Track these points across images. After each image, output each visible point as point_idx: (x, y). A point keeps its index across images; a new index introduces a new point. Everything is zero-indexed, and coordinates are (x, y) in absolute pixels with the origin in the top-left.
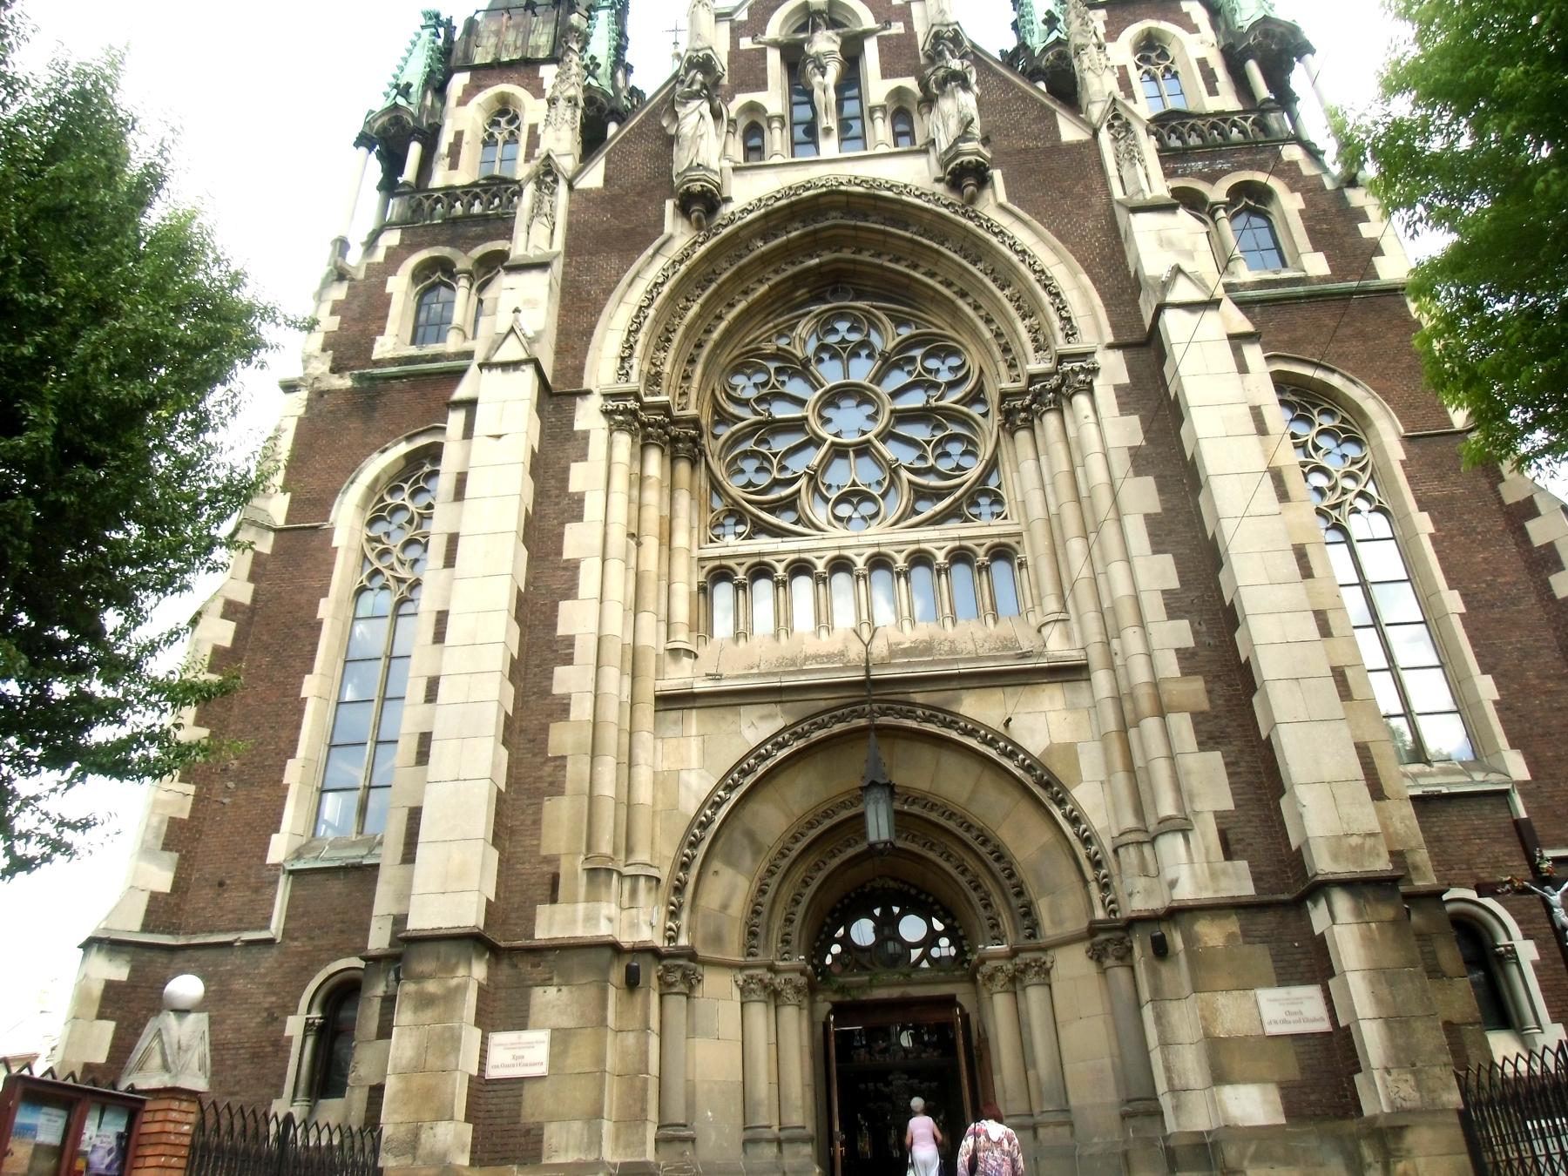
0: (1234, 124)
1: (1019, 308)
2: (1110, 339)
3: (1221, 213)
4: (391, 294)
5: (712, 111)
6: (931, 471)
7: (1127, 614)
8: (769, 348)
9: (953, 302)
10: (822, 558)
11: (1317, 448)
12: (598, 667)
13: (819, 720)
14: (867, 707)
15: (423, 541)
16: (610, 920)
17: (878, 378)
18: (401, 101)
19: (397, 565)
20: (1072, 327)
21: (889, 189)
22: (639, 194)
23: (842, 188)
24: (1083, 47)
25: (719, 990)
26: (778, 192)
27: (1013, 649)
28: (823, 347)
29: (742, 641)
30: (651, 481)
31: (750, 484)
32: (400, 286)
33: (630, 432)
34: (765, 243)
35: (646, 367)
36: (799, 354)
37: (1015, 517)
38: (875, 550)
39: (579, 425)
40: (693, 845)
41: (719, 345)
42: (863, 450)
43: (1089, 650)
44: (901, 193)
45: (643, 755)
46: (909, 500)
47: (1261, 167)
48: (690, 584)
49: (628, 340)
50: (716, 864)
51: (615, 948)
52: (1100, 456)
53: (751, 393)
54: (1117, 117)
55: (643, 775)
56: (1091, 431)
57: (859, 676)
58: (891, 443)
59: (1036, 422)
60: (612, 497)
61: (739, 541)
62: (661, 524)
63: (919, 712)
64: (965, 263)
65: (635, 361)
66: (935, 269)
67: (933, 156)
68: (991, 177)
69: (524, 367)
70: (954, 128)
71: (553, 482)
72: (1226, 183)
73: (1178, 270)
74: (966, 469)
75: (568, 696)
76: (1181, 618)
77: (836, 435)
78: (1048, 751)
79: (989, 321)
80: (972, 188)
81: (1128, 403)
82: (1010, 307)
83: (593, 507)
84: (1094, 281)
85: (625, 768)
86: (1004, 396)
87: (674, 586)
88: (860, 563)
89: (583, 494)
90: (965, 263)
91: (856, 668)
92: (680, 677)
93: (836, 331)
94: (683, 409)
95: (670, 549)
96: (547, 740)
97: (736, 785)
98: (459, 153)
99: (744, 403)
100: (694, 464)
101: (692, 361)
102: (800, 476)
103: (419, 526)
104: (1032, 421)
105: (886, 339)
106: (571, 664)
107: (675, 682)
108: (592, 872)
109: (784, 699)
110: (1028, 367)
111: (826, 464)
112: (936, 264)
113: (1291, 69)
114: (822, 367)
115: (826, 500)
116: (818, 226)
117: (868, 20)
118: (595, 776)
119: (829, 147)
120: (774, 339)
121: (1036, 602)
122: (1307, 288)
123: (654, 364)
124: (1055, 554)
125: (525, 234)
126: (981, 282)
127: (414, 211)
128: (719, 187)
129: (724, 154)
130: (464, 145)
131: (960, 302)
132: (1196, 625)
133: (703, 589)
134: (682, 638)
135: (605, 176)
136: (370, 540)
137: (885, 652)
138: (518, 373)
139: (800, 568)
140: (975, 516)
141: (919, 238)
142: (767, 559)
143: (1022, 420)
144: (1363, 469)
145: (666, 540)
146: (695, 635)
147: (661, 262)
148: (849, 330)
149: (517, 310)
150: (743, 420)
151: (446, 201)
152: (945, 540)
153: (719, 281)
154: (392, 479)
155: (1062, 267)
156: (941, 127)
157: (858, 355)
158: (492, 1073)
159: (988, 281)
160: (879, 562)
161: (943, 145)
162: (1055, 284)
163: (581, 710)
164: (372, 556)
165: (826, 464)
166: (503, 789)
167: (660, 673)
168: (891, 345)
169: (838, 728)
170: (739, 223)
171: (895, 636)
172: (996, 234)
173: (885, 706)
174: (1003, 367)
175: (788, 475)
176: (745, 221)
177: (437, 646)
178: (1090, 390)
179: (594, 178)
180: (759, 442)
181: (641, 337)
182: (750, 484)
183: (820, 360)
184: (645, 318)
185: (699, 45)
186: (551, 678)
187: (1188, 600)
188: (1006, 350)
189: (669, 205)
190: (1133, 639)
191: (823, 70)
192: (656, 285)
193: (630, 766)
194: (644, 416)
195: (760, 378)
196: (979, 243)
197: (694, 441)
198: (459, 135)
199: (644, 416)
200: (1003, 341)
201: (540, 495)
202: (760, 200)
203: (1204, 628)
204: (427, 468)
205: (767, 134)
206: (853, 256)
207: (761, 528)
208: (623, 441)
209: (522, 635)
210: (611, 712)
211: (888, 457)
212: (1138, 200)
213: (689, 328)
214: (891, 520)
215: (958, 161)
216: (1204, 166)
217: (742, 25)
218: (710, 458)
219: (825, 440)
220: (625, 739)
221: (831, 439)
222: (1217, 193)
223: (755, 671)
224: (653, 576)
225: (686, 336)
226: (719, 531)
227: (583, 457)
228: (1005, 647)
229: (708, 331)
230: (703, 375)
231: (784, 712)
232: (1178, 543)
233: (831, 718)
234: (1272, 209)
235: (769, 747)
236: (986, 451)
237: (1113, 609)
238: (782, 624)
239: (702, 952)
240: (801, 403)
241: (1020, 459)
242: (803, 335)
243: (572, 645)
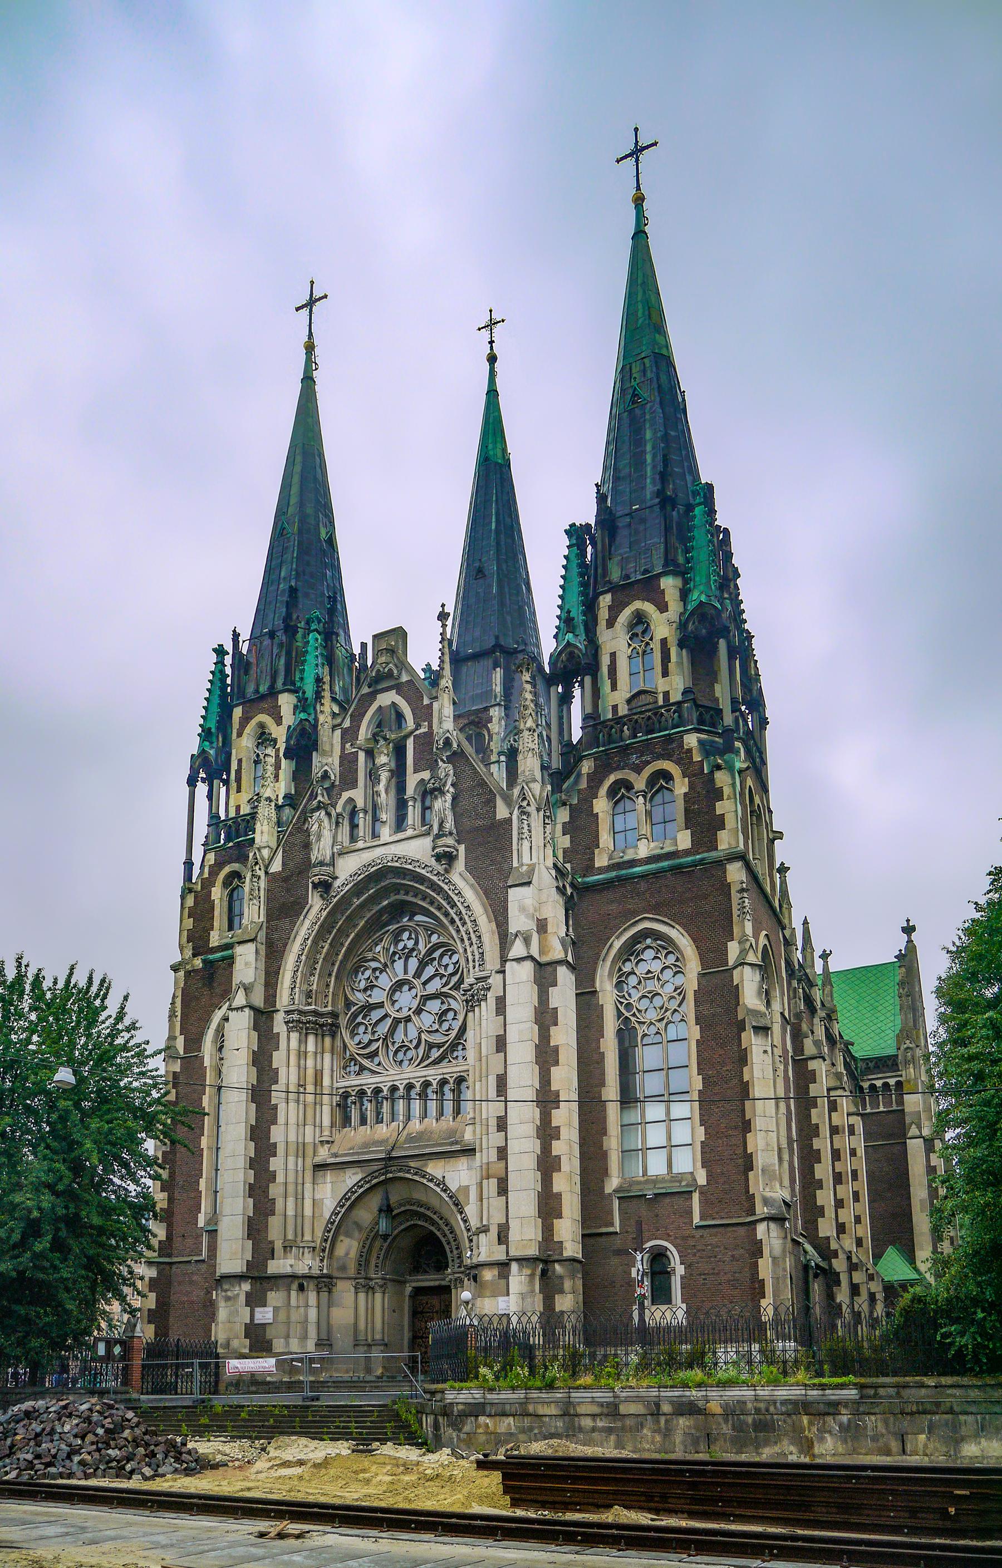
3: (641, 799)
6: (437, 1031)
11: (659, 979)
16: (291, 1266)
17: (418, 974)
25: (345, 1290)
28: (394, 953)
38: (407, 1081)
40: (329, 1232)
42: (408, 1019)
45: (308, 1195)
50: (341, 1238)
51: (294, 1277)
78: (458, 1190)
85: (300, 1201)
92: (324, 1154)
94: (326, 1007)
97: (344, 1205)
101: (330, 975)
108: (285, 1247)
133: (338, 1105)
158: (256, 1322)
163: (280, 1178)
179: (276, 867)
180: (364, 1018)
207: (363, 1068)
208: (294, 1036)
210: (291, 1179)
214: (416, 1063)
220: (300, 1187)
222: (640, 783)
227: (277, 1048)
229: (338, 955)
230: (337, 977)
239: (336, 1274)
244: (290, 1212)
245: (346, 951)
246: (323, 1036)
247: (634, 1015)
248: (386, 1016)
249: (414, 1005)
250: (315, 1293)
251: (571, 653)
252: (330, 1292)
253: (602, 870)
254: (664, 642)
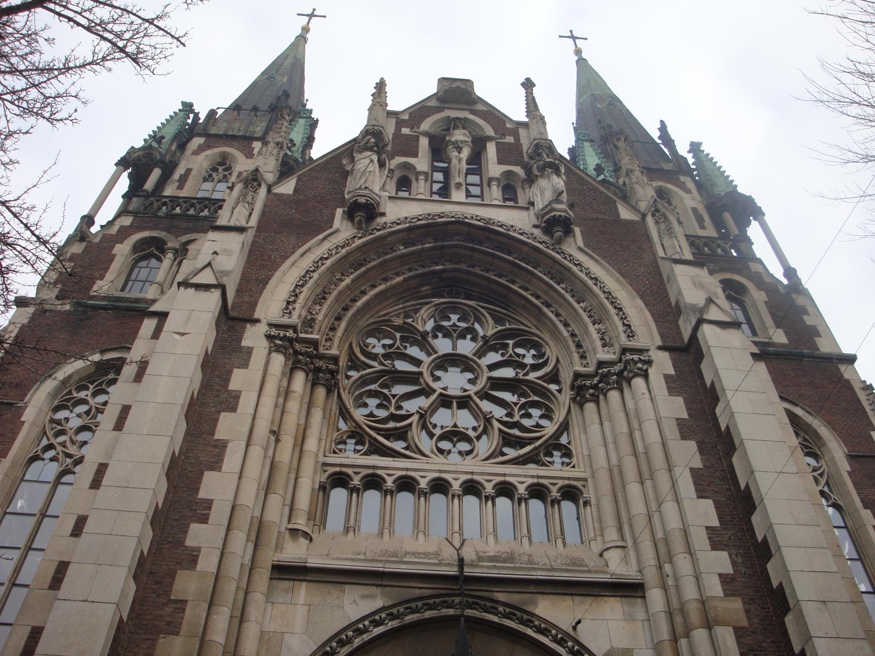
0: (719, 246)
1: (590, 317)
2: (660, 343)
4: (115, 255)
5: (379, 161)
6: (517, 425)
7: (678, 544)
8: (398, 321)
9: (539, 309)
10: (425, 477)
12: (228, 529)
13: (413, 605)
14: (457, 600)
15: (94, 428)
18: (155, 144)
19: (68, 444)
20: (632, 331)
21: (500, 226)
22: (318, 202)
23: (466, 220)
24: (632, 171)
26: (420, 215)
27: (581, 566)
28: (438, 328)
29: (351, 534)
30: (294, 394)
31: (371, 415)
32: (123, 250)
33: (285, 354)
34: (406, 248)
35: (304, 313)
36: (420, 328)
37: (582, 466)
38: (469, 477)
39: (245, 343)
41: (361, 312)
42: (464, 402)
43: (645, 571)
44: (508, 230)
45: (253, 613)
46: (498, 444)
47: (739, 272)
48: (313, 482)
49: (294, 291)
52: (655, 423)
53: (379, 350)
54: (657, 210)
55: (251, 632)
56: (646, 404)
57: (453, 571)
58: (485, 401)
59: (601, 397)
60: (263, 399)
61: (357, 455)
62: (297, 430)
63: (501, 609)
64: (551, 282)
65: (297, 306)
66: (527, 285)
67: (532, 212)
68: (573, 229)
69: (213, 290)
70: (549, 196)
71: (217, 379)
73: (710, 301)
74: (544, 427)
75: (198, 550)
76: (722, 550)
77: (444, 389)
79: (566, 325)
80: (560, 233)
81: (674, 388)
82: (584, 315)
83: (246, 404)
84: (646, 305)
85: (237, 621)
86: (577, 376)
87: (300, 480)
88: (456, 486)
89: (240, 392)
90: (551, 282)
91: (449, 565)
93: (449, 319)
94: (327, 349)
95: (301, 451)
96: (172, 584)
98: (186, 181)
99: (374, 357)
100: (329, 391)
101: (339, 318)
102: (412, 415)
103: (94, 417)
104: (598, 397)
105: (488, 329)
106: (206, 523)
107: (291, 556)
109: (384, 583)
110: (598, 356)
111: (433, 409)
112: (529, 283)
113: (749, 223)
114: (435, 341)
115: (431, 435)
116: (445, 243)
117: (489, 131)
118: (210, 623)
119: (458, 195)
120: (402, 316)
121: (598, 533)
122: (774, 349)
123: (311, 313)
124: (615, 496)
125: (229, 213)
126: (562, 296)
127: (146, 208)
128: (378, 204)
129: (383, 188)
130: (191, 178)
131: (545, 309)
132: (734, 556)
134: (301, 522)
135: (295, 188)
136: (52, 421)
137: (474, 557)
138: (207, 294)
139: (407, 484)
140: (549, 462)
141: (519, 262)
142: (379, 472)
143: (590, 395)
144: (821, 475)
145: (299, 443)
146: (312, 523)
147: (327, 245)
148: (459, 320)
149: (215, 253)
150: (371, 367)
151: (170, 204)
152: (526, 476)
153: (368, 266)
154: (82, 379)
155: (624, 293)
156: (539, 195)
157: (465, 338)
159: (568, 296)
160: (472, 488)
161: (539, 205)
162: (618, 302)
163: (207, 563)
164: (50, 434)
165: (433, 409)
166: (125, 618)
167: (278, 547)
168: (490, 333)
169: (428, 614)
170: (389, 230)
171: (481, 547)
172: (576, 265)
173: (471, 600)
174: (576, 357)
175: (403, 412)
176: (393, 229)
177: (92, 491)
178: (646, 376)
179: (287, 188)
180: (383, 386)
181: (305, 290)
182: (371, 415)
183: (435, 337)
184: (310, 278)
185: (375, 123)
186: (186, 532)
187: (727, 537)
188: (579, 346)
189: (339, 212)
190: (683, 563)
191: (460, 150)
192: (321, 259)
193: (241, 621)
194: (298, 346)
195: (388, 342)
196: (562, 270)
197: (333, 373)
198: (189, 171)
199: (298, 346)
200: (577, 339)
201: (205, 387)
202: (406, 218)
203: (740, 561)
204: (111, 376)
205: (414, 184)
206: (467, 268)
208: (278, 360)
209: (168, 491)
210: (233, 569)
211: (484, 410)
212: (677, 257)
213: (340, 293)
215: (552, 214)
217: (404, 121)
218: (341, 391)
219: (434, 391)
220: (241, 596)
221: (439, 391)
223: (362, 557)
224: (285, 467)
225: (337, 300)
226: (341, 446)
227: (245, 365)
228: (574, 564)
229: (354, 301)
230: (346, 330)
231: (384, 595)
232: (716, 492)
233: (424, 605)
234: (746, 299)
235: (367, 623)
236: (559, 416)
237: (666, 540)
238: (387, 524)
240: (417, 362)
241: (587, 423)
242: (425, 317)
243: (210, 508)
245: (368, 303)
249: (472, 389)
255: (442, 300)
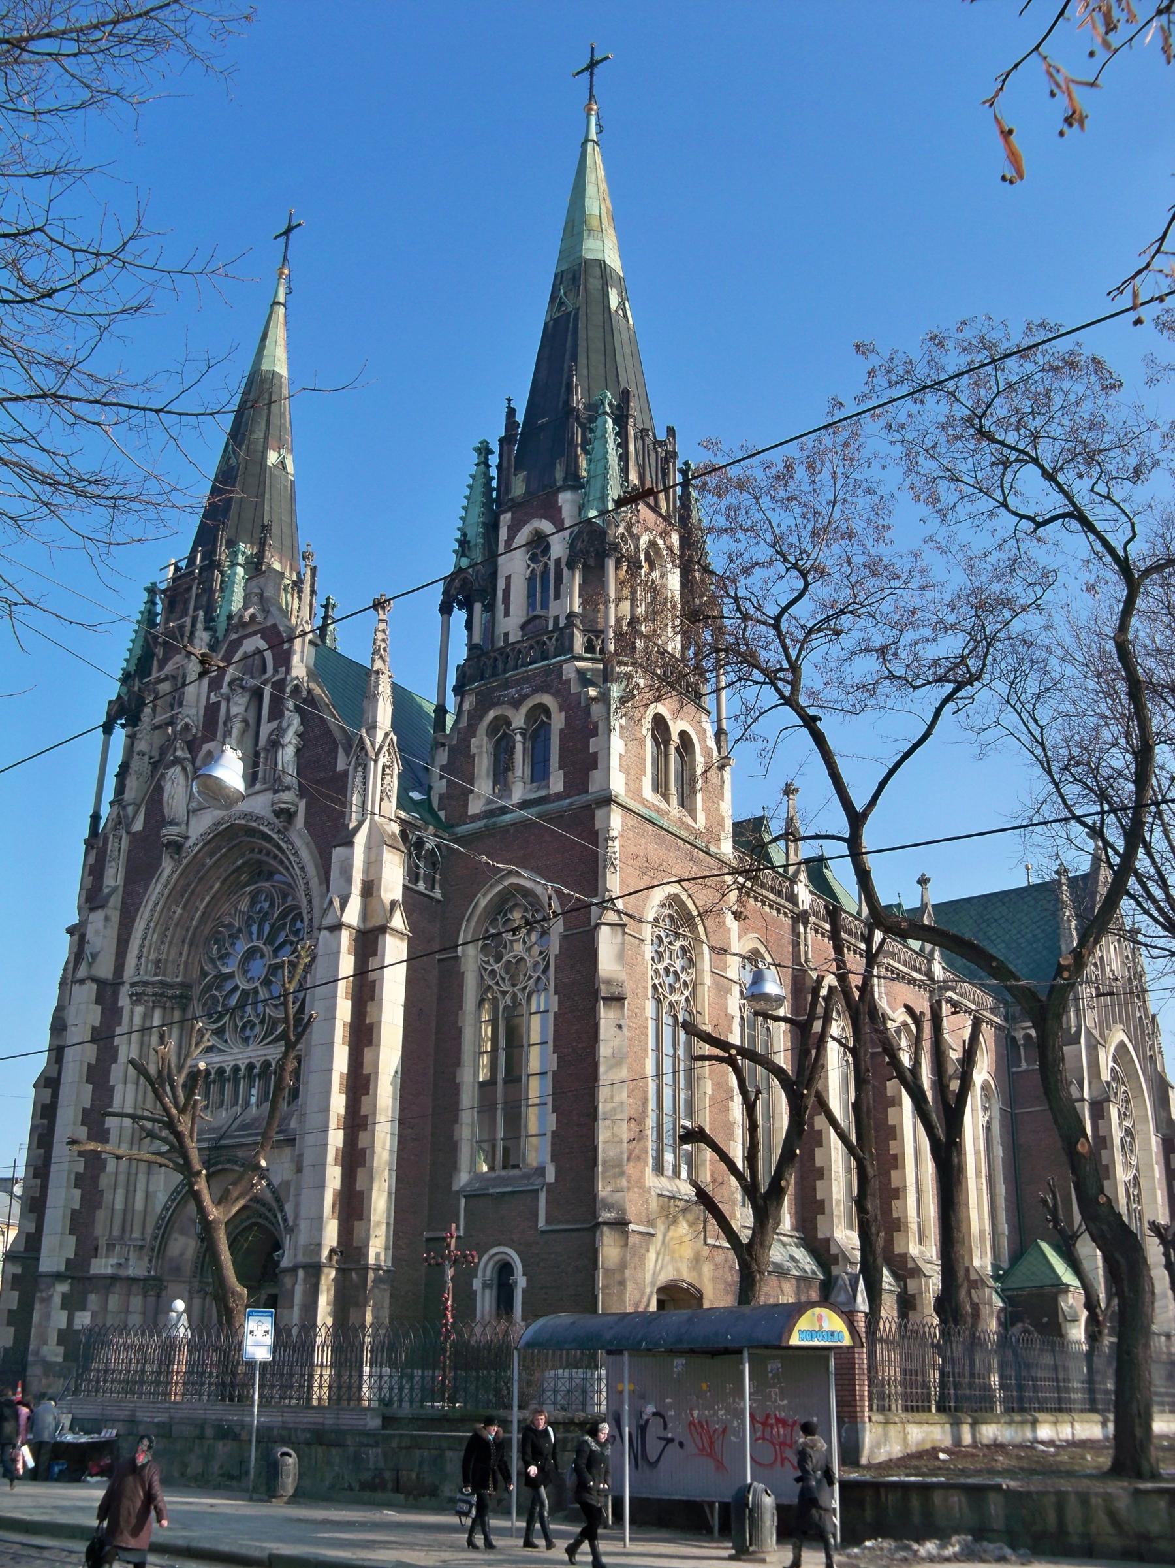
3: (519, 738)
33: (141, 1004)
40: (159, 1228)
50: (175, 1235)
55: (140, 1196)
72: (524, 710)
78: (280, 1184)
100: (184, 1009)
101: (183, 942)
144: (544, 959)
179: (138, 826)
216: (517, 692)
221: (242, 987)
222: (518, 719)
229: (192, 919)
230: (191, 945)
244: (119, 1206)
246: (173, 1009)
247: (497, 983)
248: (236, 987)
250: (140, 1298)
251: (464, 580)
252: (158, 1296)
253: (476, 818)
254: (558, 561)
255: (252, 887)
